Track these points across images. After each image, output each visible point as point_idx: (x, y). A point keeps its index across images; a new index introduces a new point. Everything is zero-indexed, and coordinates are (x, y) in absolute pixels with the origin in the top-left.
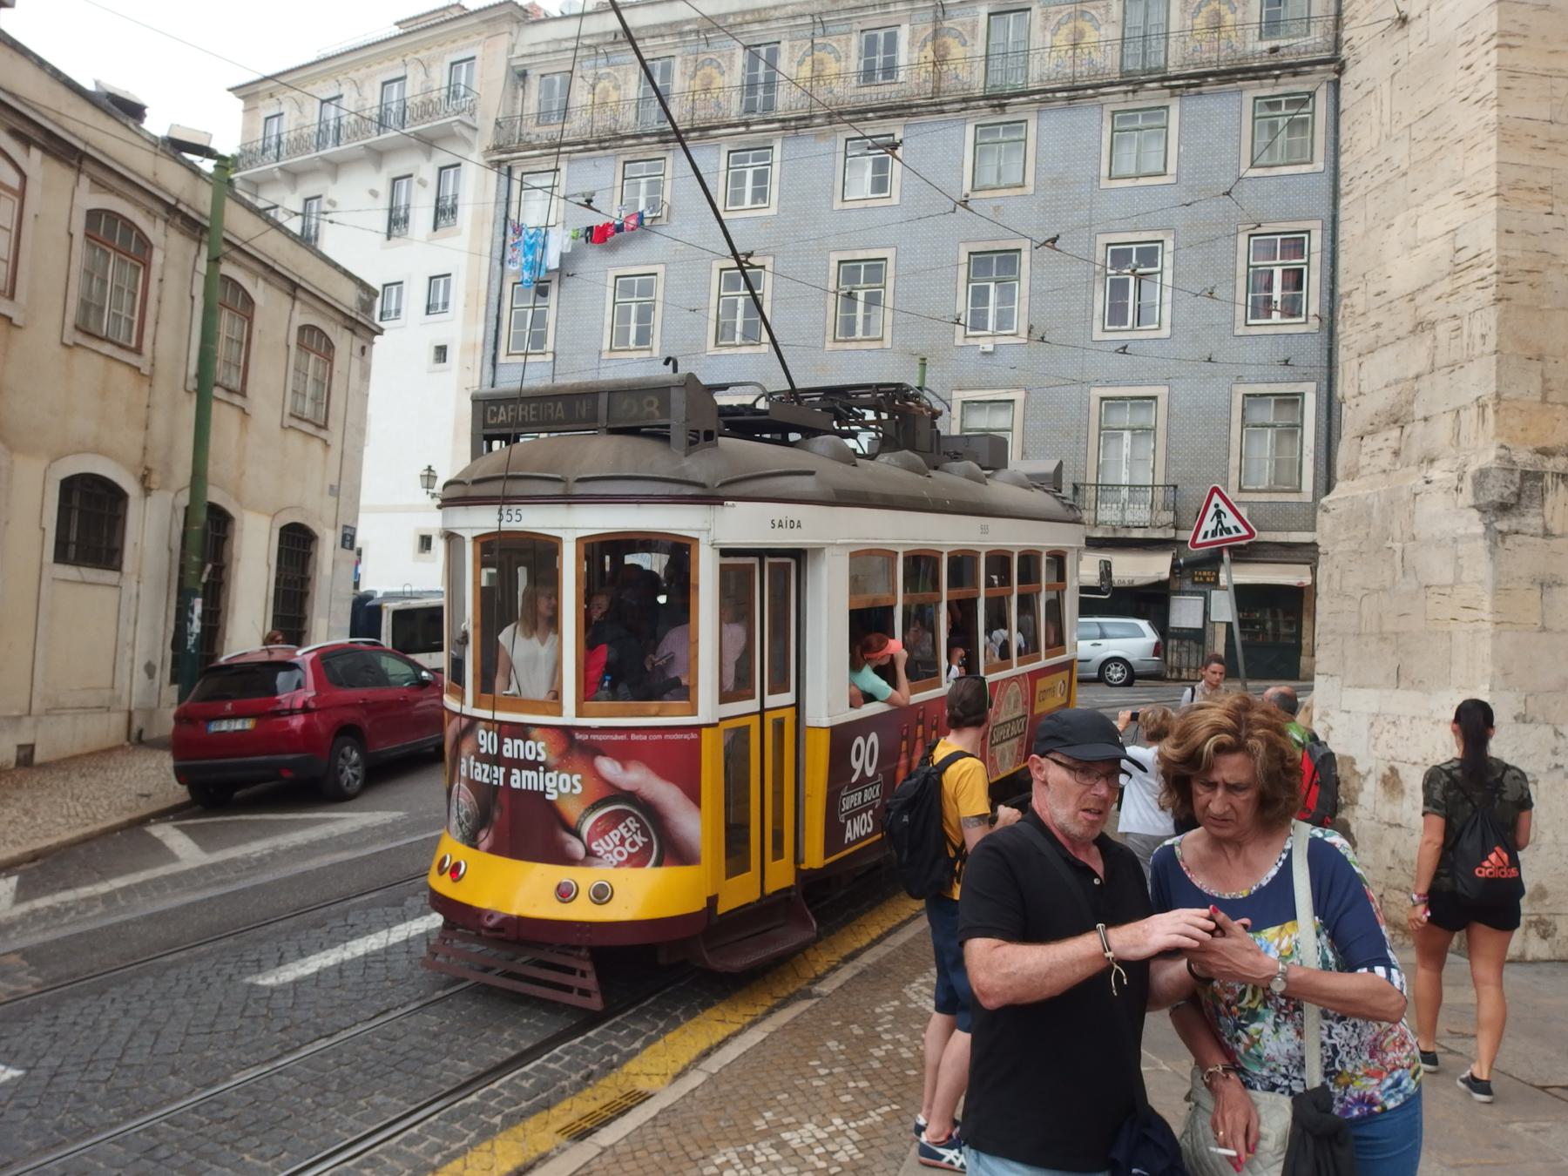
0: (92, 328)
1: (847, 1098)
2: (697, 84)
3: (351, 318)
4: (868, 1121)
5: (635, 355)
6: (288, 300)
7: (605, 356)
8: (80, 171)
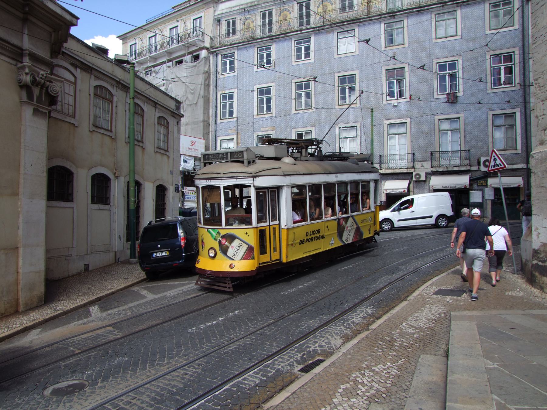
0: (97, 124)
1: (390, 357)
2: (281, 18)
3: (174, 112)
4: (399, 363)
5: (266, 116)
6: (154, 108)
7: (255, 117)
8: (91, 74)
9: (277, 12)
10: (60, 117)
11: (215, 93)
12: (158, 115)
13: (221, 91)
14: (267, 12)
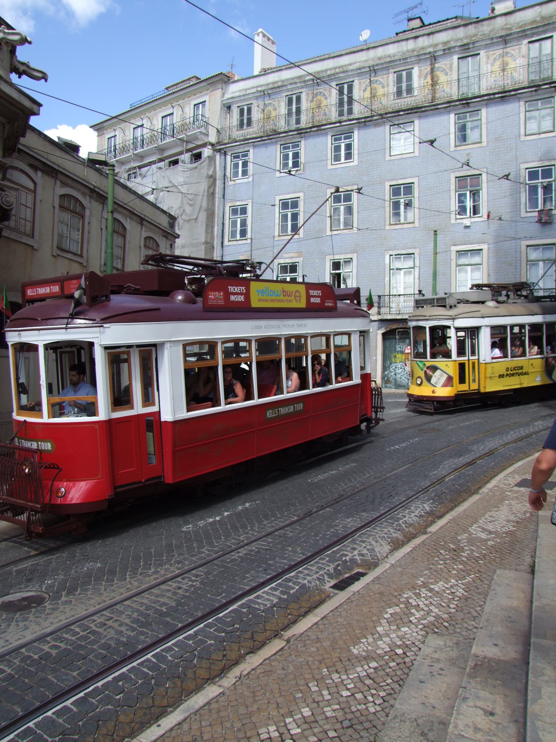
0: (63, 247)
1: (455, 572)
2: (313, 105)
3: (166, 231)
4: (467, 580)
6: (140, 226)
7: (276, 239)
8: (56, 179)
9: (308, 97)
10: (13, 236)
11: (222, 205)
12: (145, 234)
13: (230, 202)
14: (294, 97)
